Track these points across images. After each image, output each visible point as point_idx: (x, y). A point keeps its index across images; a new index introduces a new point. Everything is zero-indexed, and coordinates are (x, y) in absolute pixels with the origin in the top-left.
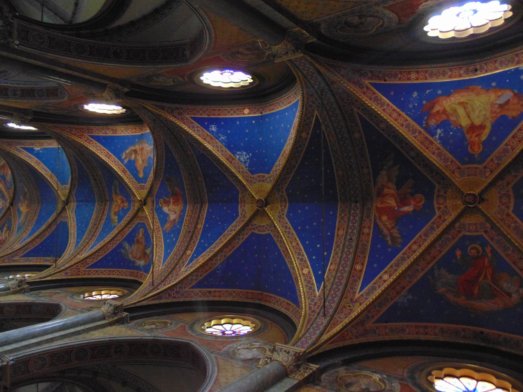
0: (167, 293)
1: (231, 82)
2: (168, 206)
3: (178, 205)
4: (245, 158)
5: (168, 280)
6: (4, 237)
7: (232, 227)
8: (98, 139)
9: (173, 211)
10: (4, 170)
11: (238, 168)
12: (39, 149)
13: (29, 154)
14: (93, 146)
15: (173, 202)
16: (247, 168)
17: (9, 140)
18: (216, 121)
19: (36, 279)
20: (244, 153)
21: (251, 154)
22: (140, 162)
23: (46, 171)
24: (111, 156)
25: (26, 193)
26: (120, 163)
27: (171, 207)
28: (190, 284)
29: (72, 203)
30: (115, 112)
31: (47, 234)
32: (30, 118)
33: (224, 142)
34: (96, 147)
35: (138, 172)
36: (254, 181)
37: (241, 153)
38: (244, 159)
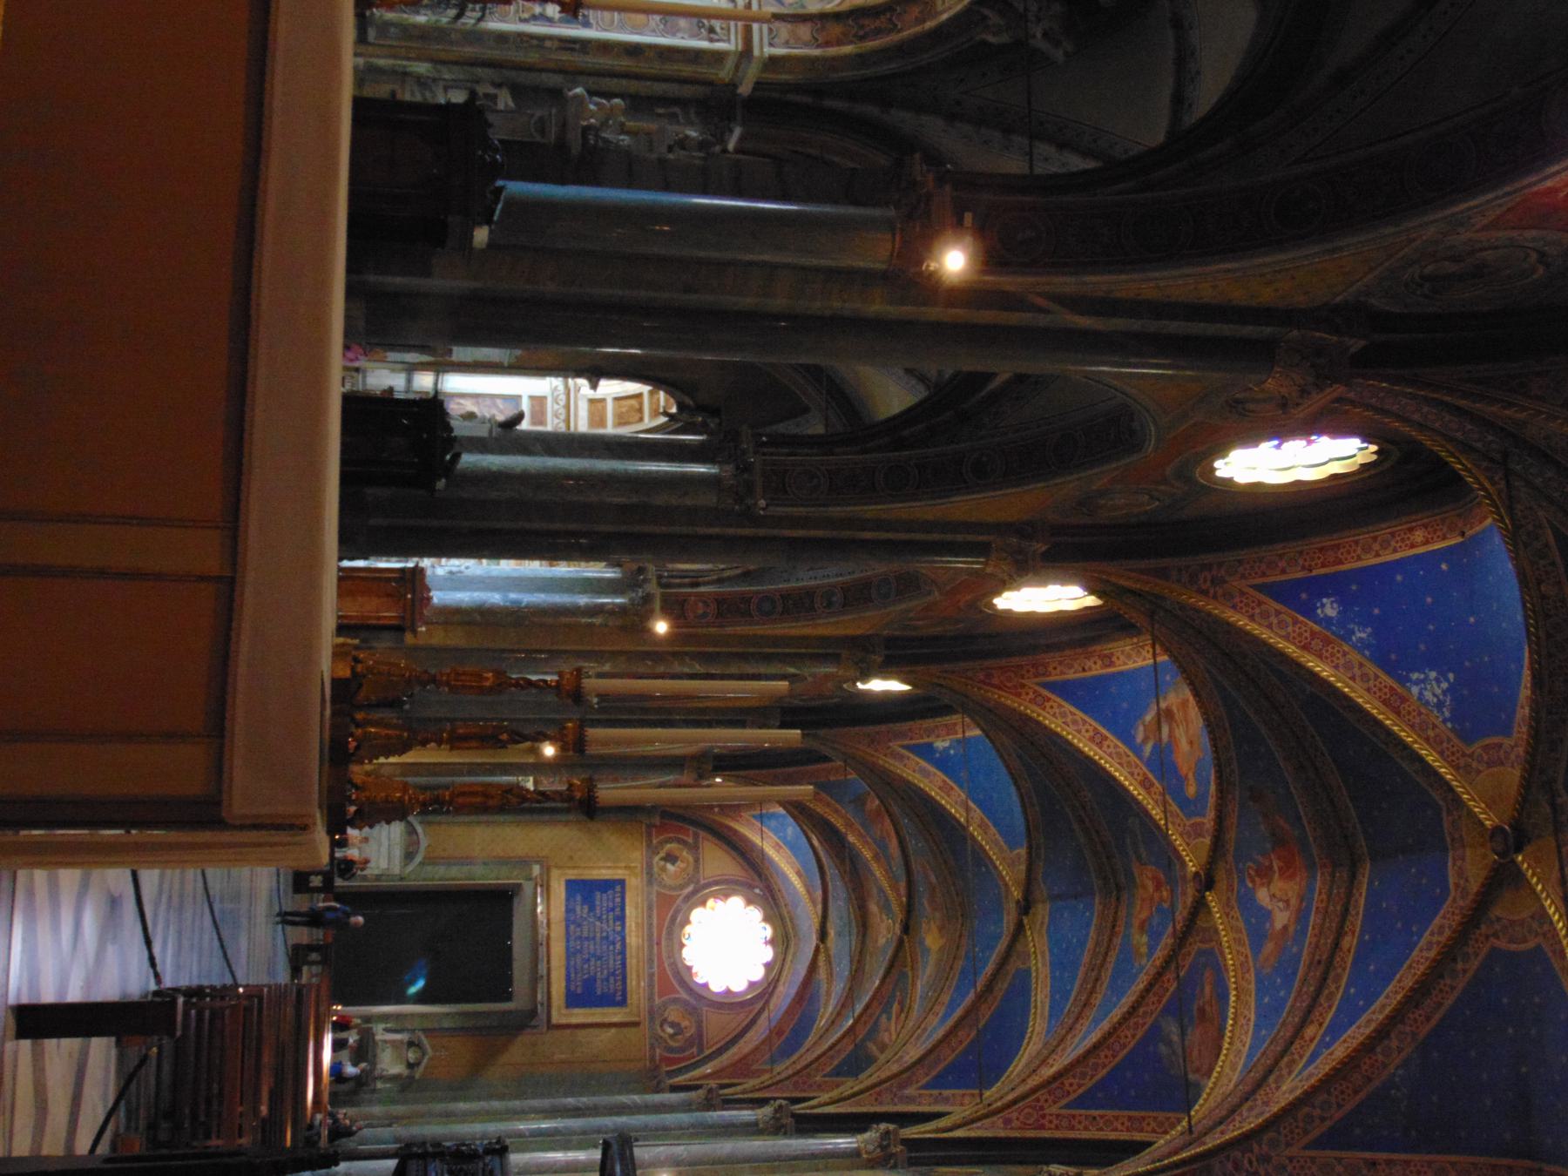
0: (1228, 1158)
1: (1331, 460)
2: (1269, 884)
3: (1292, 877)
4: (1438, 691)
5: (1238, 1118)
7: (1432, 934)
8: (1066, 690)
9: (1281, 900)
11: (1420, 729)
12: (947, 744)
13: (923, 763)
14: (1054, 715)
15: (1280, 869)
16: (1449, 725)
17: (870, 729)
18: (1334, 585)
20: (1433, 674)
21: (1451, 676)
22: (1184, 745)
24: (1106, 738)
26: (1133, 758)
27: (1278, 885)
28: (1306, 1132)
29: (1040, 906)
33: (1368, 646)
34: (1064, 715)
35: (1182, 780)
36: (1474, 764)
37: (1422, 676)
38: (1434, 695)
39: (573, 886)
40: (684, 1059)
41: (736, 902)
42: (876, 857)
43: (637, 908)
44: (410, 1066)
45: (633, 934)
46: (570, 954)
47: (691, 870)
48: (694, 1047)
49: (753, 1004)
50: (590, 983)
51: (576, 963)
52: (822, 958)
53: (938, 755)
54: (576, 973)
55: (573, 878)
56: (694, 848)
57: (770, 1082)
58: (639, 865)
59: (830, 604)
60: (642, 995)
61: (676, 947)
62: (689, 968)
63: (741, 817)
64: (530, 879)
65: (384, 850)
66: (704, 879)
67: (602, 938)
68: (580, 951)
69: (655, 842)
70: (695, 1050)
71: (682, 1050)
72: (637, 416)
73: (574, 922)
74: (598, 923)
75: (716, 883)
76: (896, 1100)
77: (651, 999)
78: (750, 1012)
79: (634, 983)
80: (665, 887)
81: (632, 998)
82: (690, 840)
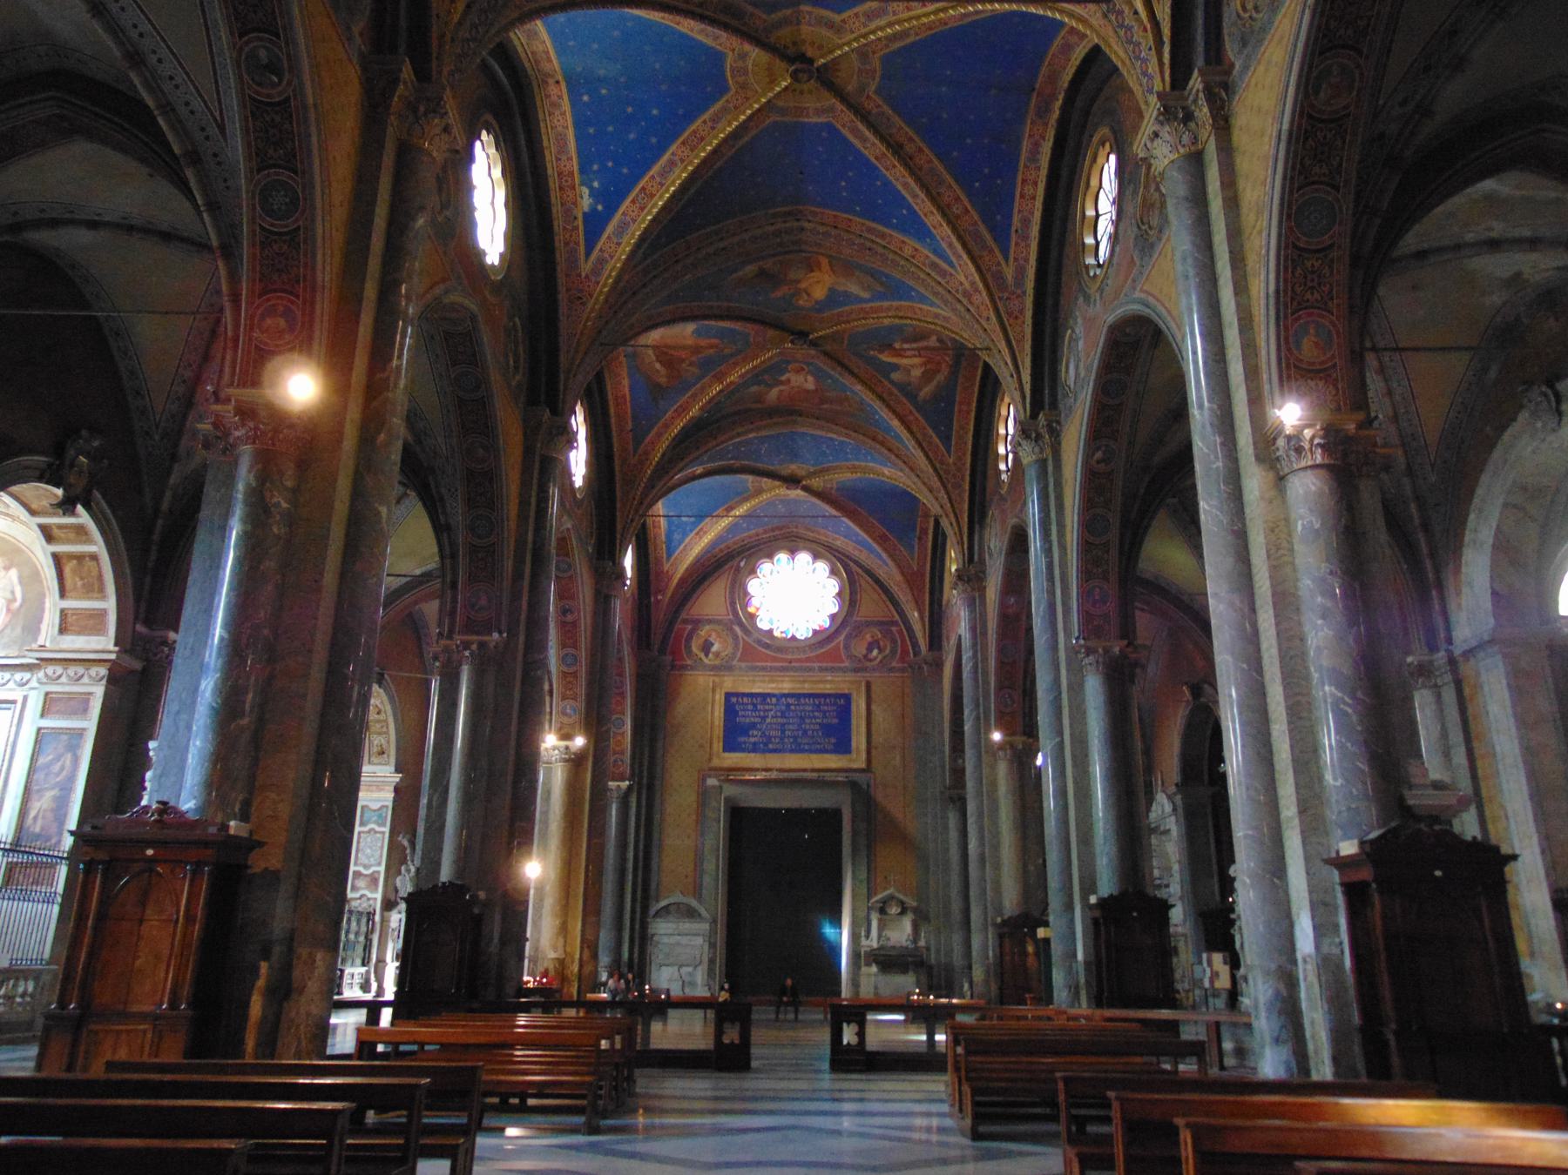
6: (917, 361)
10: (683, 361)
12: (585, 191)
13: (610, 229)
17: (562, 296)
19: (1161, 64)
23: (672, 164)
25: (762, 273)
30: (497, 172)
31: (928, 158)
32: (407, 72)
39: (730, 745)
40: (903, 641)
41: (753, 586)
42: (719, 378)
44: (903, 912)
46: (798, 749)
48: (892, 628)
50: (827, 730)
52: (816, 483)
53: (600, 207)
56: (697, 623)
57: (952, 515)
58: (711, 679)
59: (273, 67)
61: (794, 644)
62: (815, 632)
64: (721, 787)
65: (684, 940)
68: (795, 738)
69: (689, 662)
70: (894, 629)
71: (894, 641)
72: (90, 564)
74: (768, 720)
75: (733, 604)
76: (1019, 291)
77: (845, 670)
79: (828, 686)
80: (734, 654)
82: (690, 627)
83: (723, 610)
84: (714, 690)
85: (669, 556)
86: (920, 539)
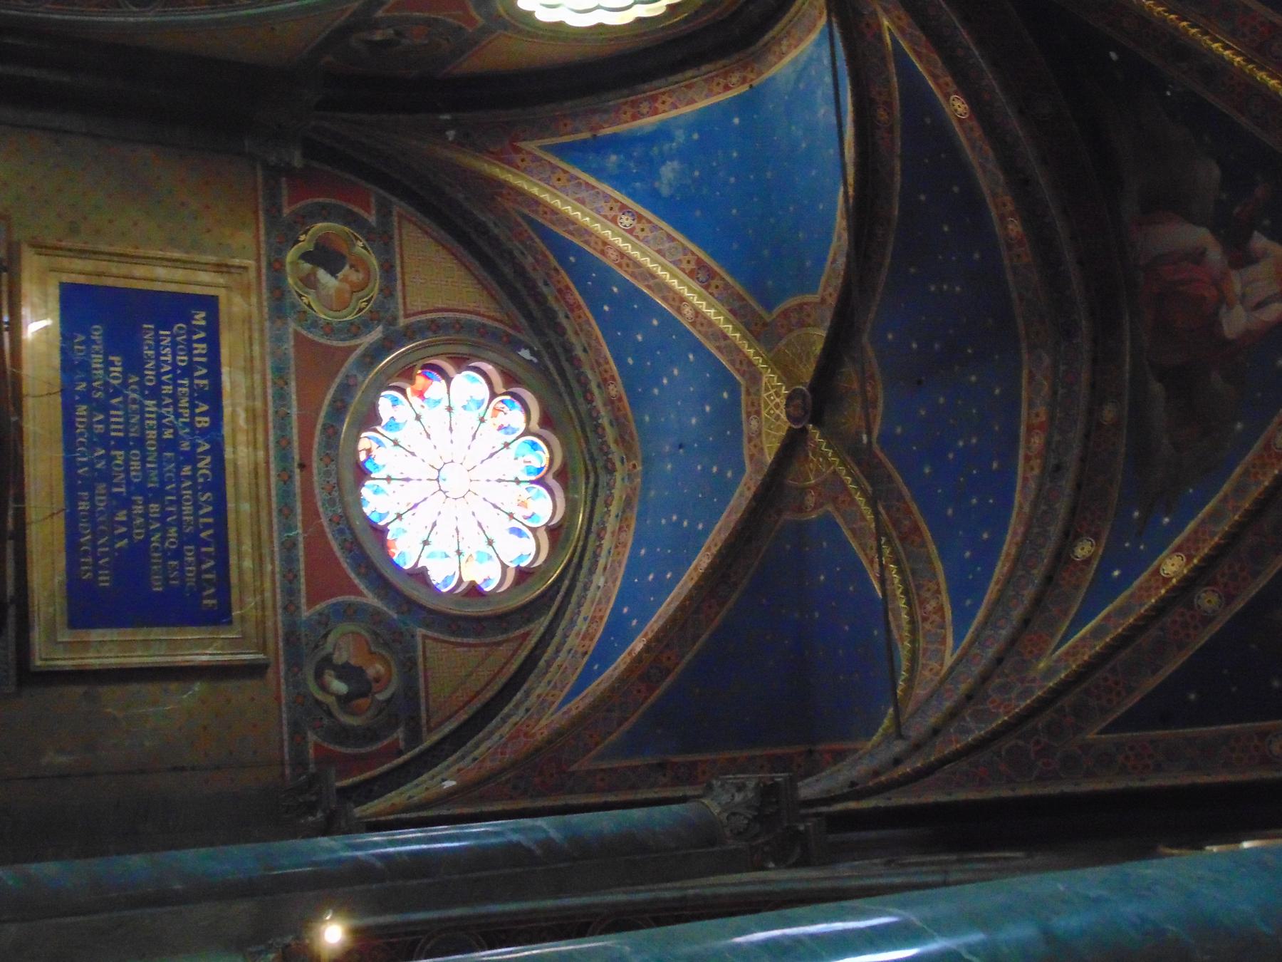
43: (249, 370)
45: (242, 438)
46: (74, 484)
47: (375, 289)
49: (529, 620)
51: (93, 506)
54: (96, 535)
55: (82, 280)
56: (382, 239)
58: (251, 263)
60: (268, 594)
62: (380, 533)
63: (518, 150)
66: (406, 316)
67: (164, 445)
69: (286, 211)
70: (400, 734)
71: (370, 735)
73: (86, 397)
74: (150, 404)
77: (290, 607)
78: (525, 636)
79: (247, 564)
80: (315, 324)
81: (245, 605)
82: (372, 219)
83: (417, 303)
84: (221, 268)
85: (560, 151)
86: (661, 766)
